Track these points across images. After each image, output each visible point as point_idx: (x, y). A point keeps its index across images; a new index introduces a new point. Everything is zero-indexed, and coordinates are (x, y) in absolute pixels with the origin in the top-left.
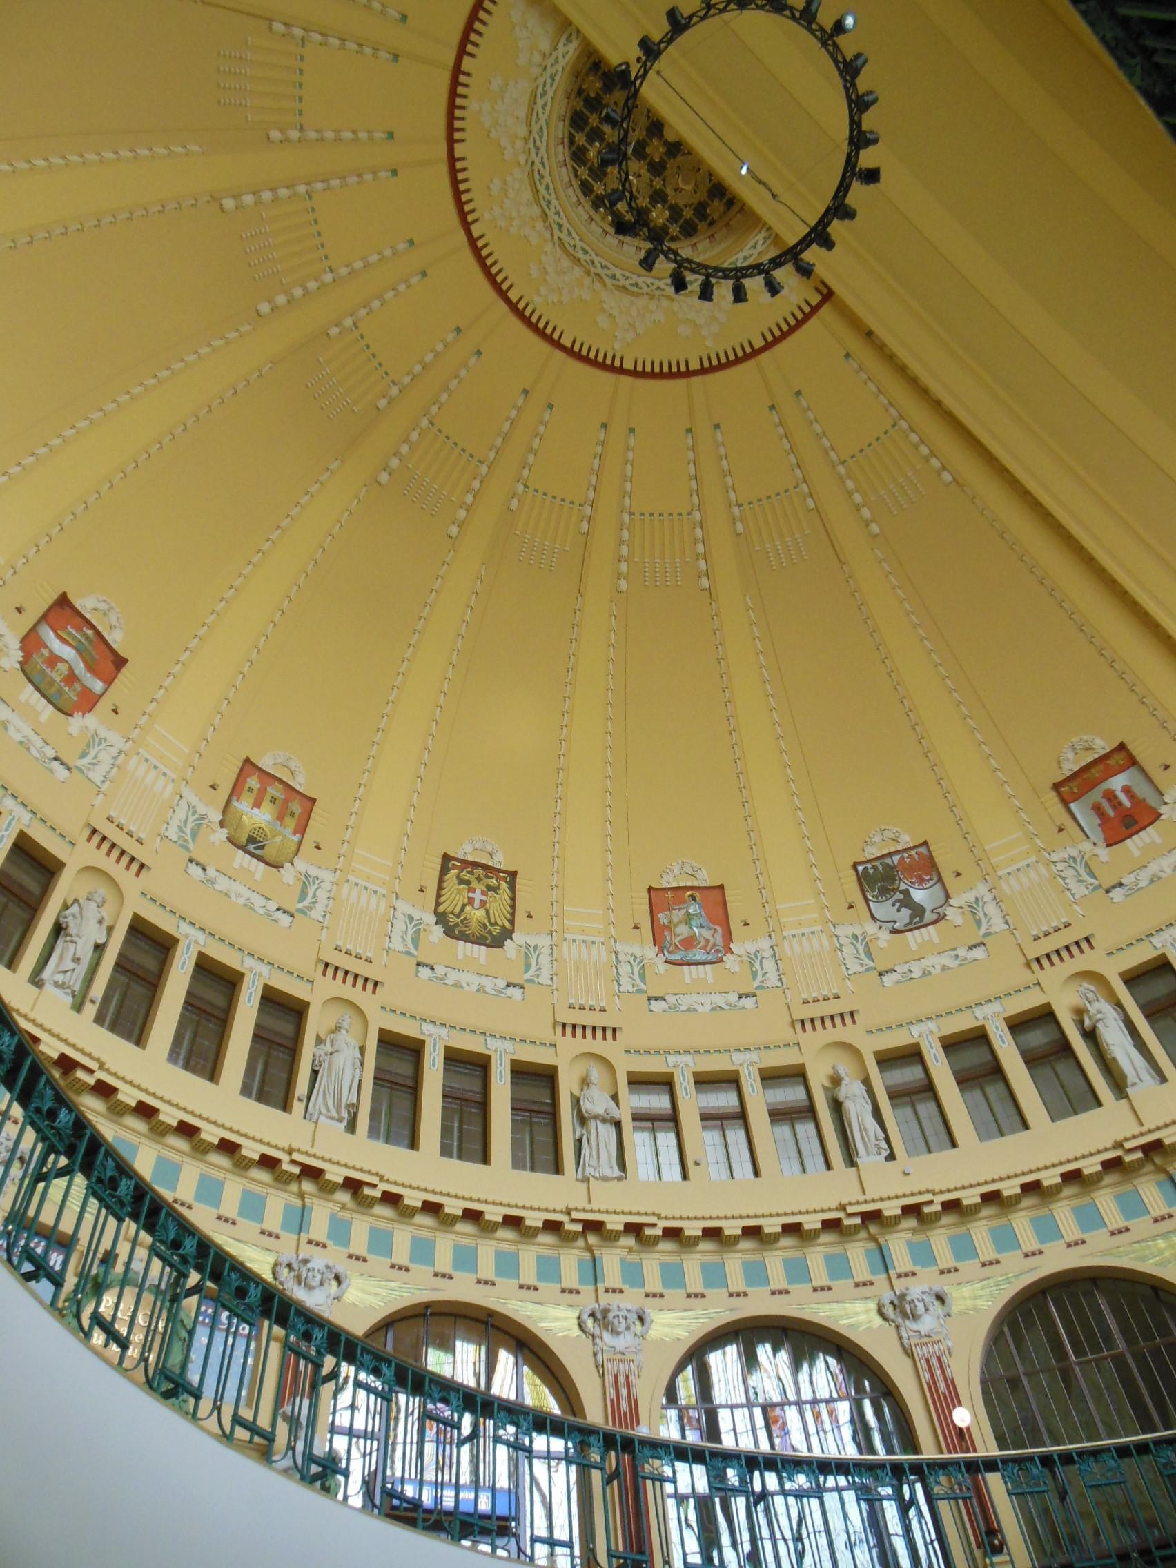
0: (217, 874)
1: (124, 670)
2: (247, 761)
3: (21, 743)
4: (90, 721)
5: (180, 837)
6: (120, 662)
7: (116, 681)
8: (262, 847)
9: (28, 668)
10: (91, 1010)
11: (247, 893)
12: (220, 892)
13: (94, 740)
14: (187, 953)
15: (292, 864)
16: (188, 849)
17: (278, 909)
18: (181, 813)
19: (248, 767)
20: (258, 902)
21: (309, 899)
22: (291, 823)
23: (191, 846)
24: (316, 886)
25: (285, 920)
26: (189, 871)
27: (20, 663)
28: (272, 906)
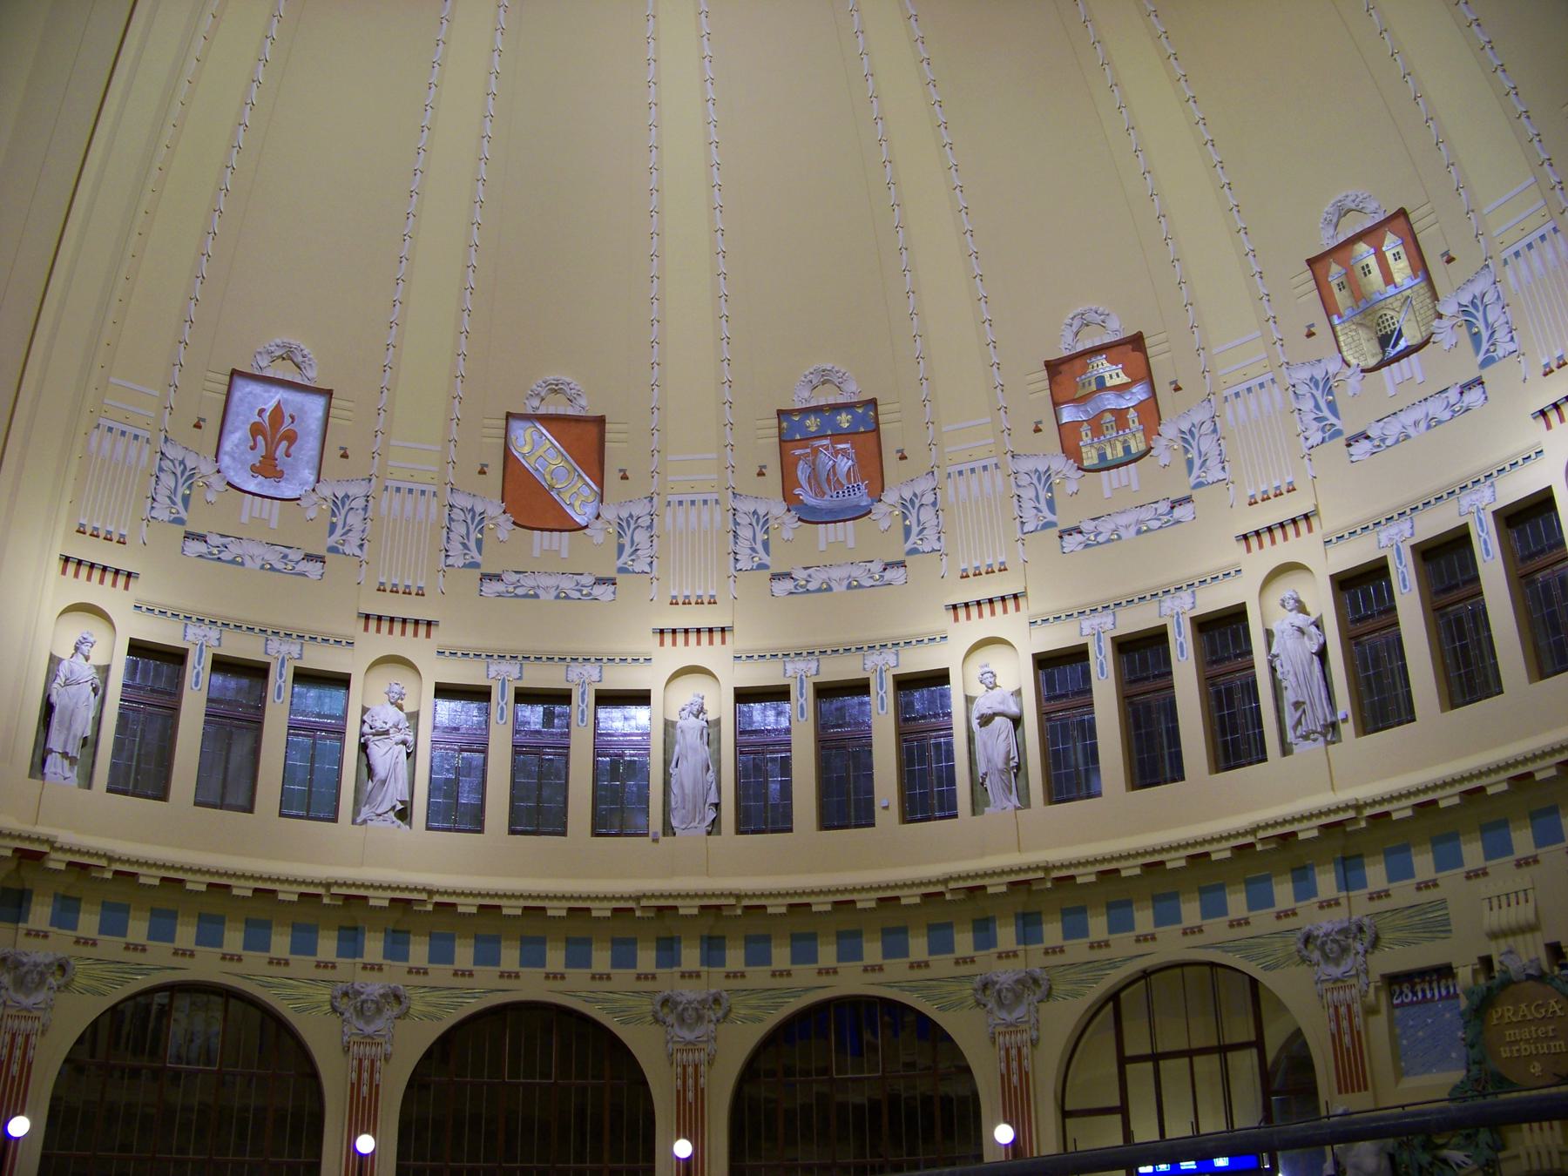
0: (1381, 424)
1: (1147, 342)
2: (1310, 262)
3: (1139, 532)
4: (1169, 430)
5: (1323, 429)
6: (1136, 342)
7: (1151, 361)
8: (1400, 335)
9: (1086, 463)
10: (1347, 729)
11: (1418, 413)
12: (1397, 442)
13: (1187, 437)
14: (1401, 563)
15: (1440, 316)
16: (1339, 433)
17: (1462, 393)
18: (1308, 405)
19: (1318, 266)
20: (1436, 408)
21: (1485, 335)
22: (1401, 270)
23: (1339, 425)
24: (1481, 309)
25: (1474, 396)
26: (1354, 459)
27: (1079, 468)
28: (1453, 395)
